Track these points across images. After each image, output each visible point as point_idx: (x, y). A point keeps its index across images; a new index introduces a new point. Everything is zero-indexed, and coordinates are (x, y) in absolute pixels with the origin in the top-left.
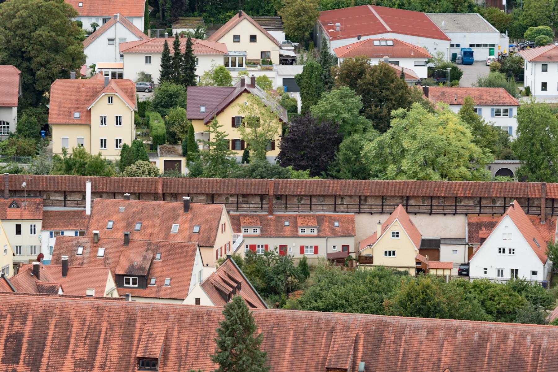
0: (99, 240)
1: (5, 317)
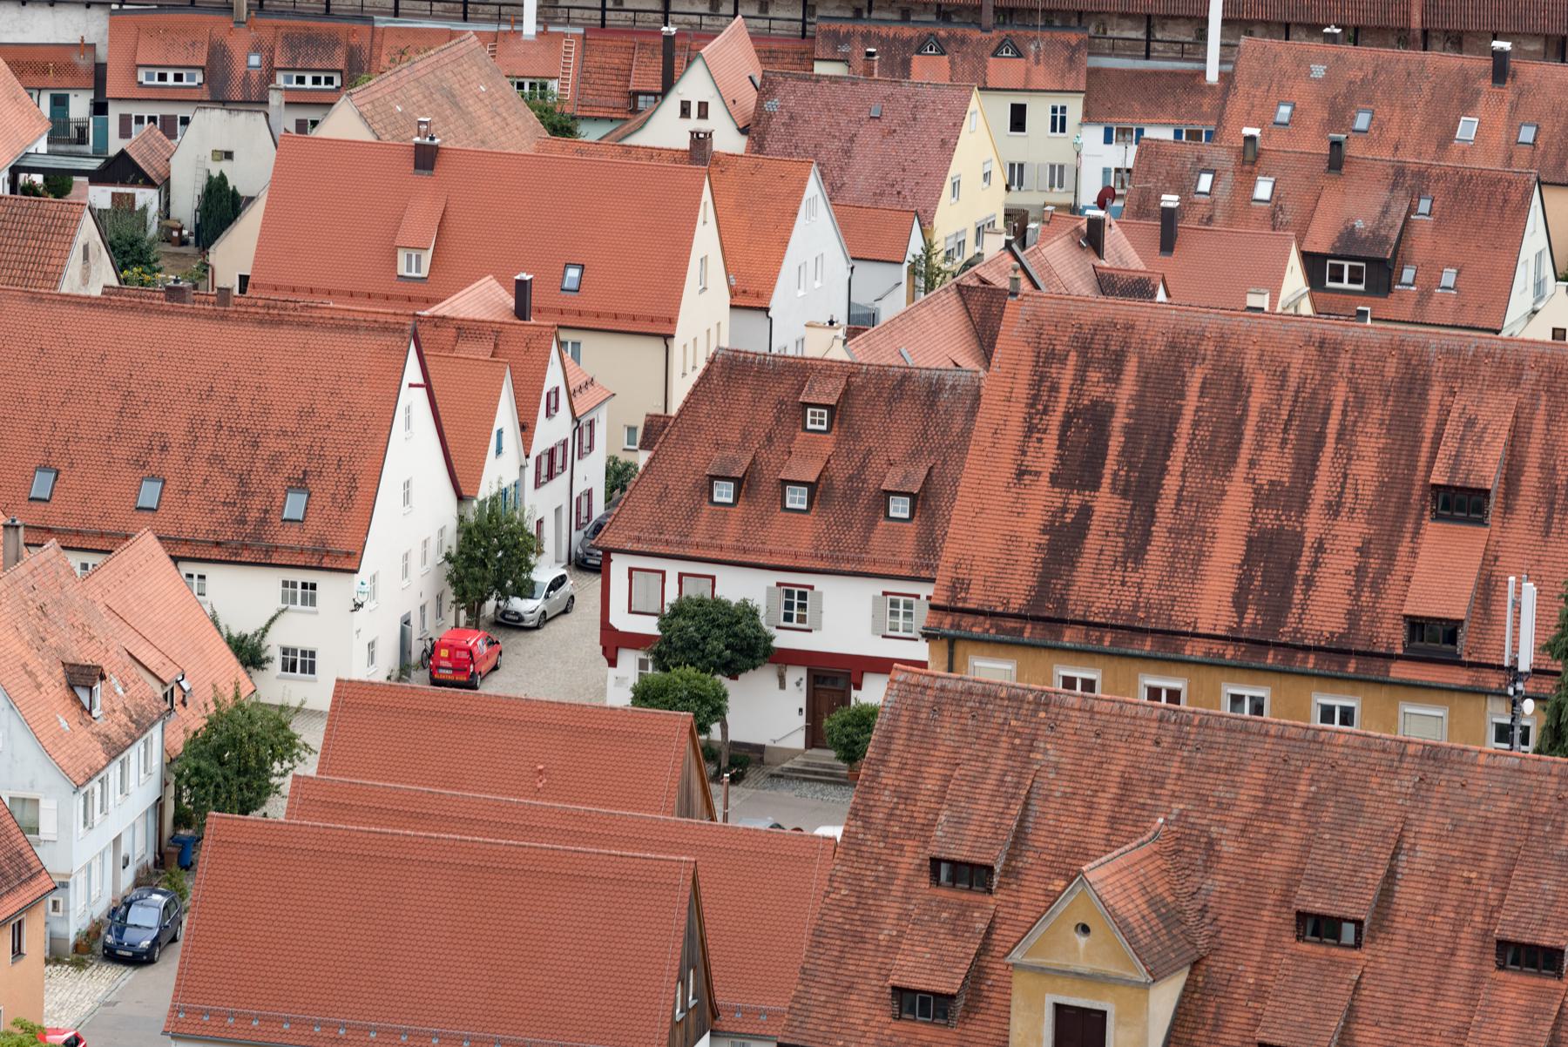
0: (1257, 155)
1: (1063, 360)
